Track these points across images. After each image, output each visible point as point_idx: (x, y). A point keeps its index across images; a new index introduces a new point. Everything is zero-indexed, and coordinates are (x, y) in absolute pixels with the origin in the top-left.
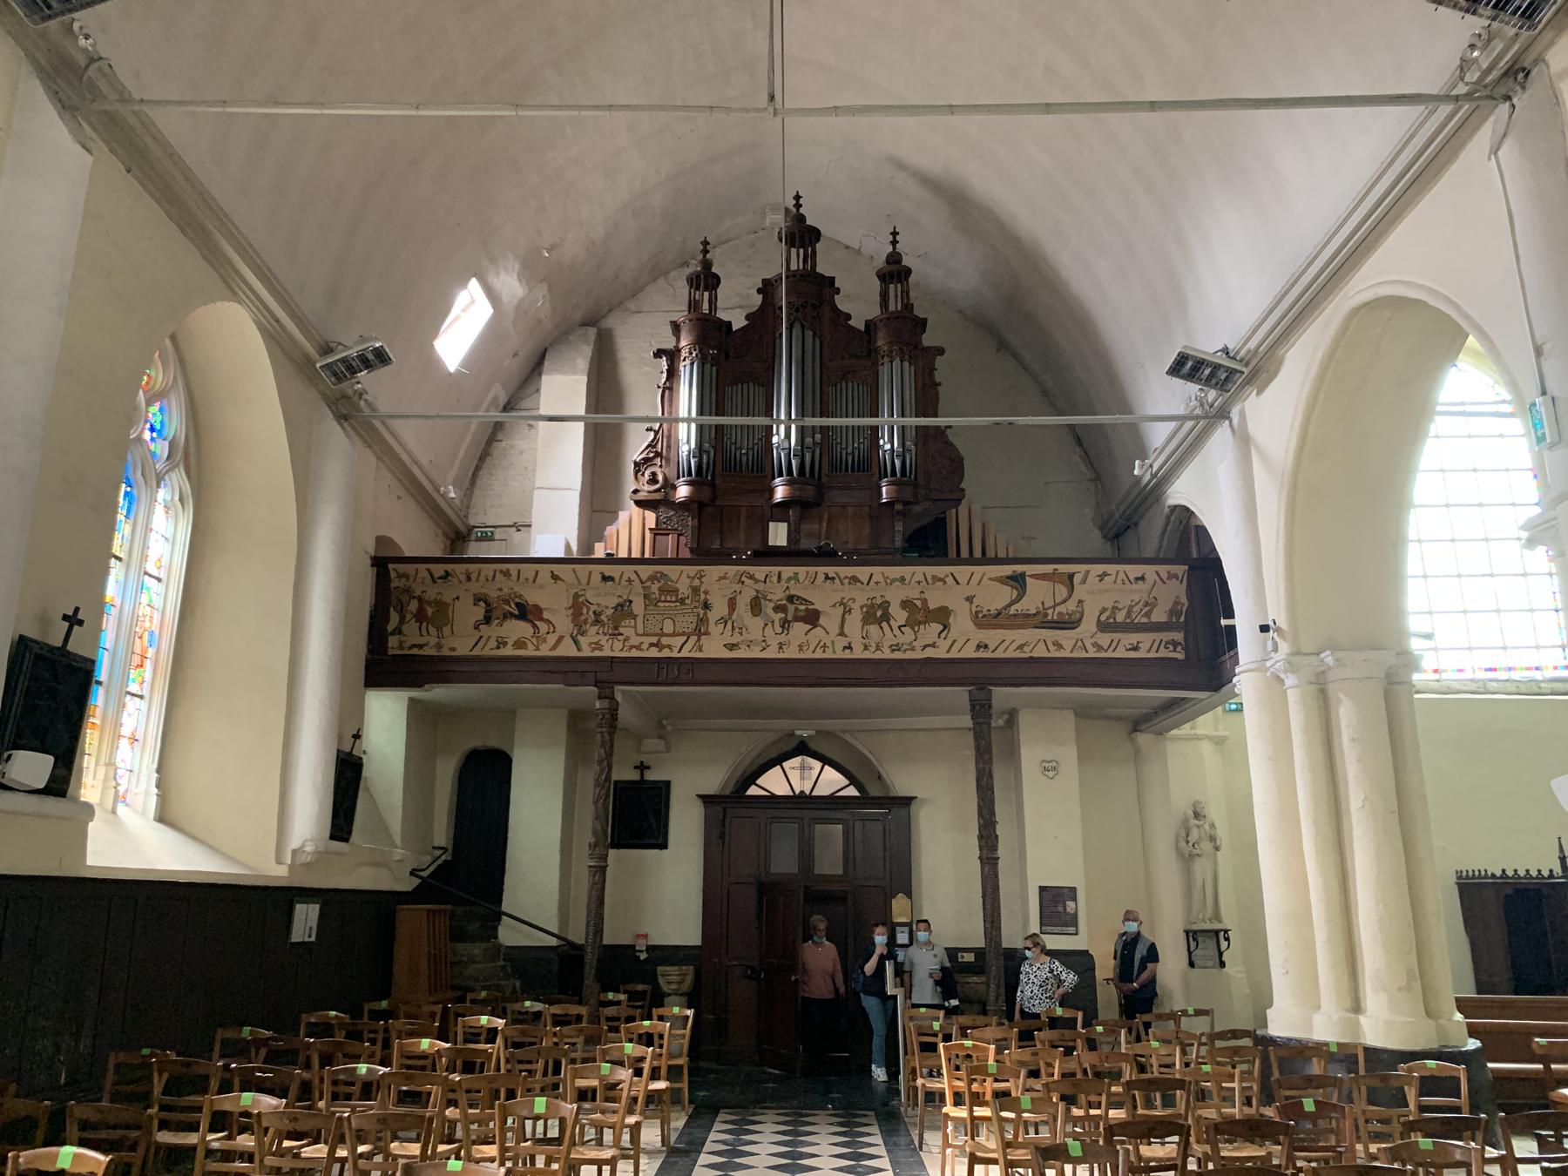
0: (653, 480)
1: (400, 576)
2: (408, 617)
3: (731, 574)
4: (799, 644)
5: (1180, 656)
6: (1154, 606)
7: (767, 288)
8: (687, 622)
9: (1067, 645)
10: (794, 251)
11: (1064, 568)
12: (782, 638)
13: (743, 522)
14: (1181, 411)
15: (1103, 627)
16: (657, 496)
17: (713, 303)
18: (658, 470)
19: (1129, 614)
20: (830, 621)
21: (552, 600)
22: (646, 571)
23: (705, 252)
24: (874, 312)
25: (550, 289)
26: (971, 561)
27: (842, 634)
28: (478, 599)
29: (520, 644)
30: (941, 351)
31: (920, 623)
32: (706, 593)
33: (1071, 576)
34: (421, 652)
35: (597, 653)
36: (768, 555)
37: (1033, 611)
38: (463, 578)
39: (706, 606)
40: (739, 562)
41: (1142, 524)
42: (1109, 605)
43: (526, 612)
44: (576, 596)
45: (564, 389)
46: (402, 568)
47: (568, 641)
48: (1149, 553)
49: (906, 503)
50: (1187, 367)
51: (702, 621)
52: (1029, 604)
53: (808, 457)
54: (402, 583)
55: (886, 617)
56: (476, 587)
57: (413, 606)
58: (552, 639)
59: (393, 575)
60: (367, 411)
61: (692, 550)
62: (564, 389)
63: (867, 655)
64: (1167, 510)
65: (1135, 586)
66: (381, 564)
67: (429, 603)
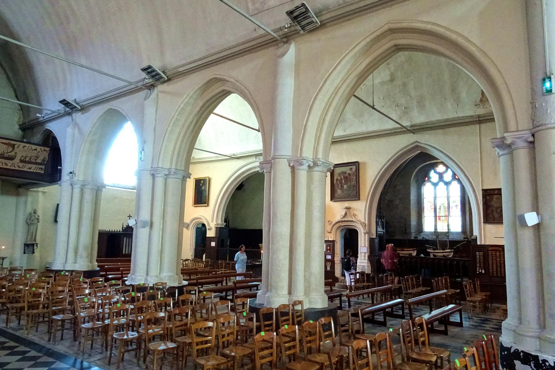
5: (43, 172)
9: (9, 165)
15: (21, 161)
19: (30, 159)
33: (14, 145)
42: (24, 155)
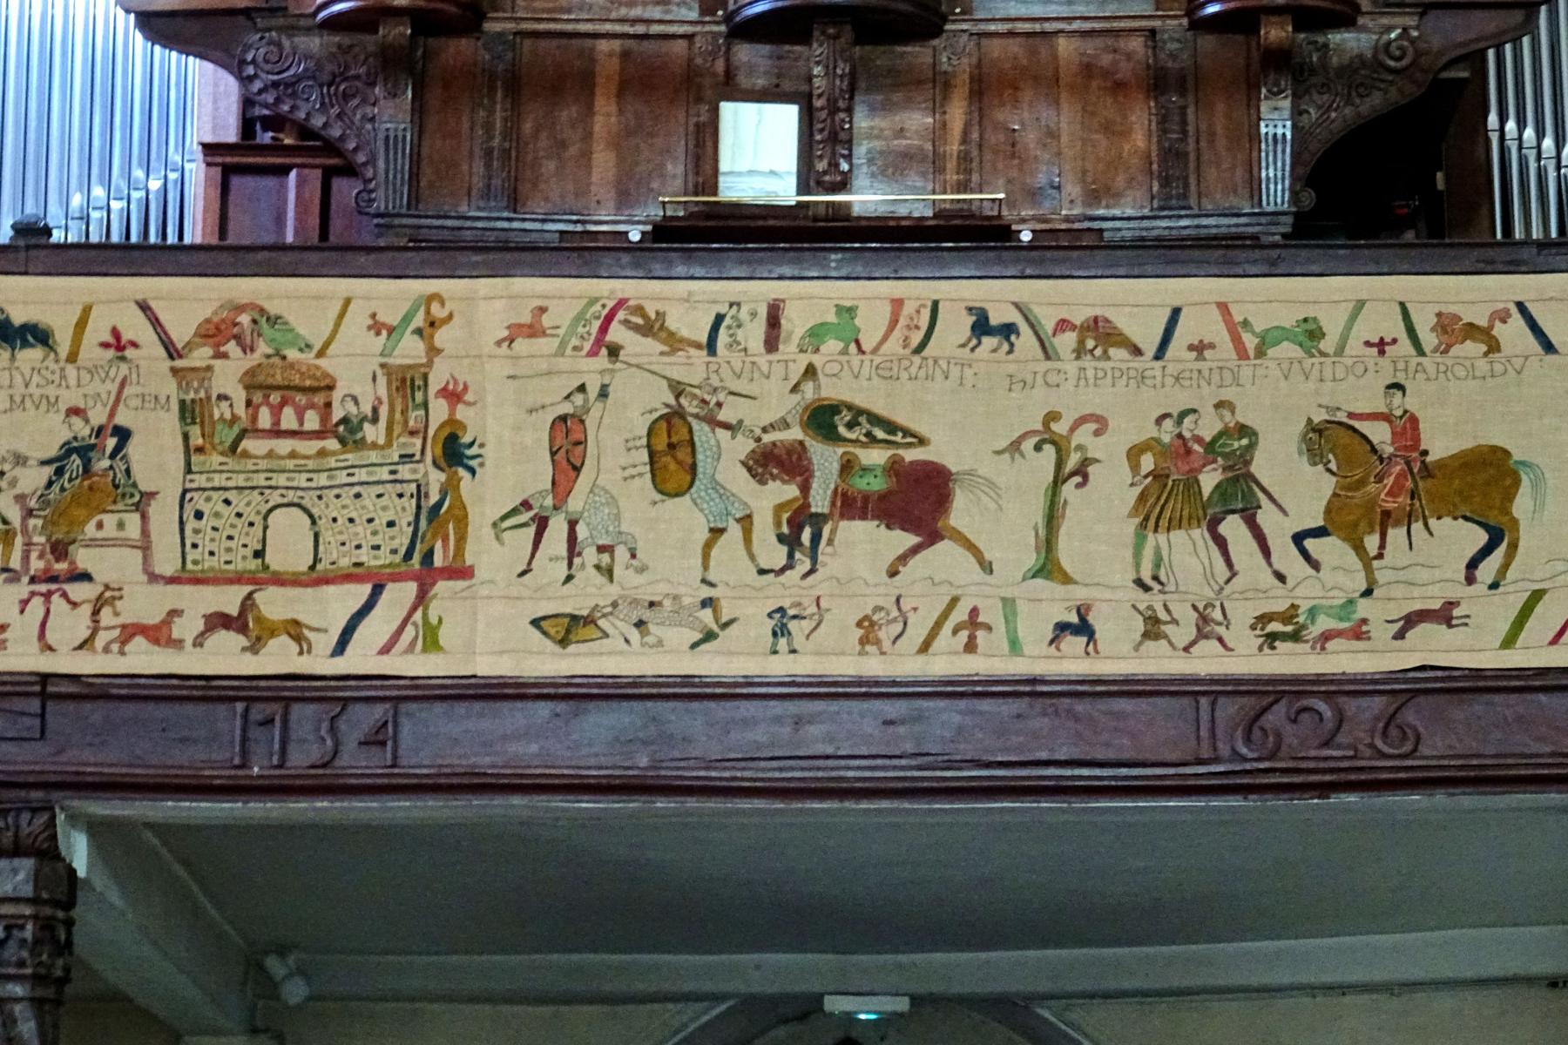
3: (559, 317)
8: (374, 523)
12: (790, 589)
22: (188, 301)
27: (1048, 568)
31: (1386, 520)
39: (454, 452)
51: (438, 517)
55: (1241, 494)
63: (1160, 662)
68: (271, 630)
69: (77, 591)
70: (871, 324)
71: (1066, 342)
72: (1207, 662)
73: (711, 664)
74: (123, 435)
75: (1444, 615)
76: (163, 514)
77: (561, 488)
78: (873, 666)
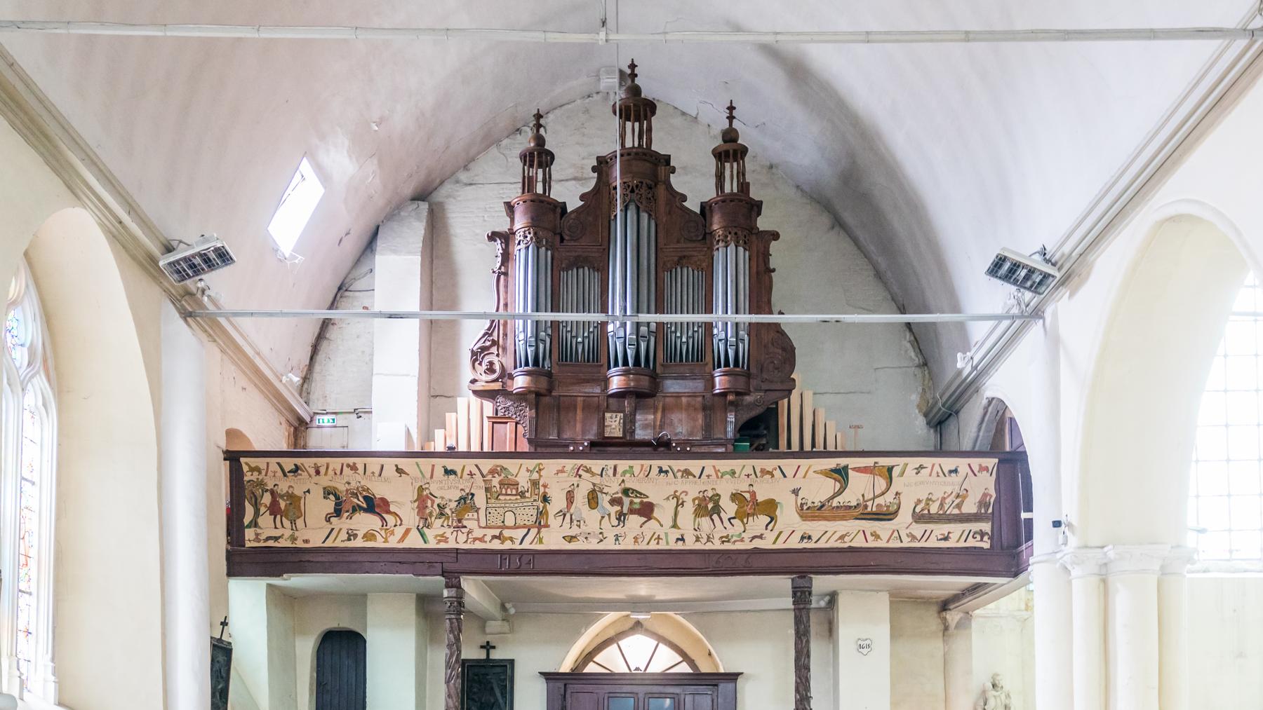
0: (491, 370)
1: (252, 470)
2: (263, 510)
3: (568, 468)
4: (634, 535)
6: (965, 497)
7: (602, 165)
8: (528, 514)
9: (884, 535)
10: (629, 124)
11: (885, 461)
12: (619, 530)
13: (579, 412)
14: (999, 311)
15: (919, 518)
16: (497, 386)
17: (547, 182)
18: (495, 360)
19: (942, 505)
20: (664, 513)
21: (400, 494)
22: (486, 465)
23: (539, 126)
24: (710, 193)
25: (380, 163)
26: (802, 454)
27: (675, 526)
28: (328, 492)
29: (369, 536)
30: (775, 236)
32: (545, 486)
34: (276, 544)
35: (443, 546)
36: (602, 446)
37: (854, 503)
38: (312, 472)
39: (545, 499)
40: (575, 455)
41: (962, 415)
42: (924, 497)
43: (374, 505)
44: (421, 489)
45: (397, 273)
46: (254, 462)
47: (414, 534)
48: (967, 445)
49: (738, 394)
50: (1005, 269)
51: (542, 514)
52: (850, 497)
53: (643, 346)
54: (255, 476)
55: (717, 509)
56: (325, 481)
57: (267, 499)
58: (399, 531)
59: (245, 468)
60: (211, 308)
61: (530, 441)
62: (397, 273)
63: (698, 546)
64: (985, 402)
65: (948, 479)
66: (233, 457)
67: (282, 497)
68: (506, 539)
69: (464, 530)
70: (636, 470)
71: (679, 474)
72: (709, 546)
73: (601, 547)
74: (473, 495)
75: (761, 537)
76: (482, 512)
77: (569, 507)
78: (637, 547)
